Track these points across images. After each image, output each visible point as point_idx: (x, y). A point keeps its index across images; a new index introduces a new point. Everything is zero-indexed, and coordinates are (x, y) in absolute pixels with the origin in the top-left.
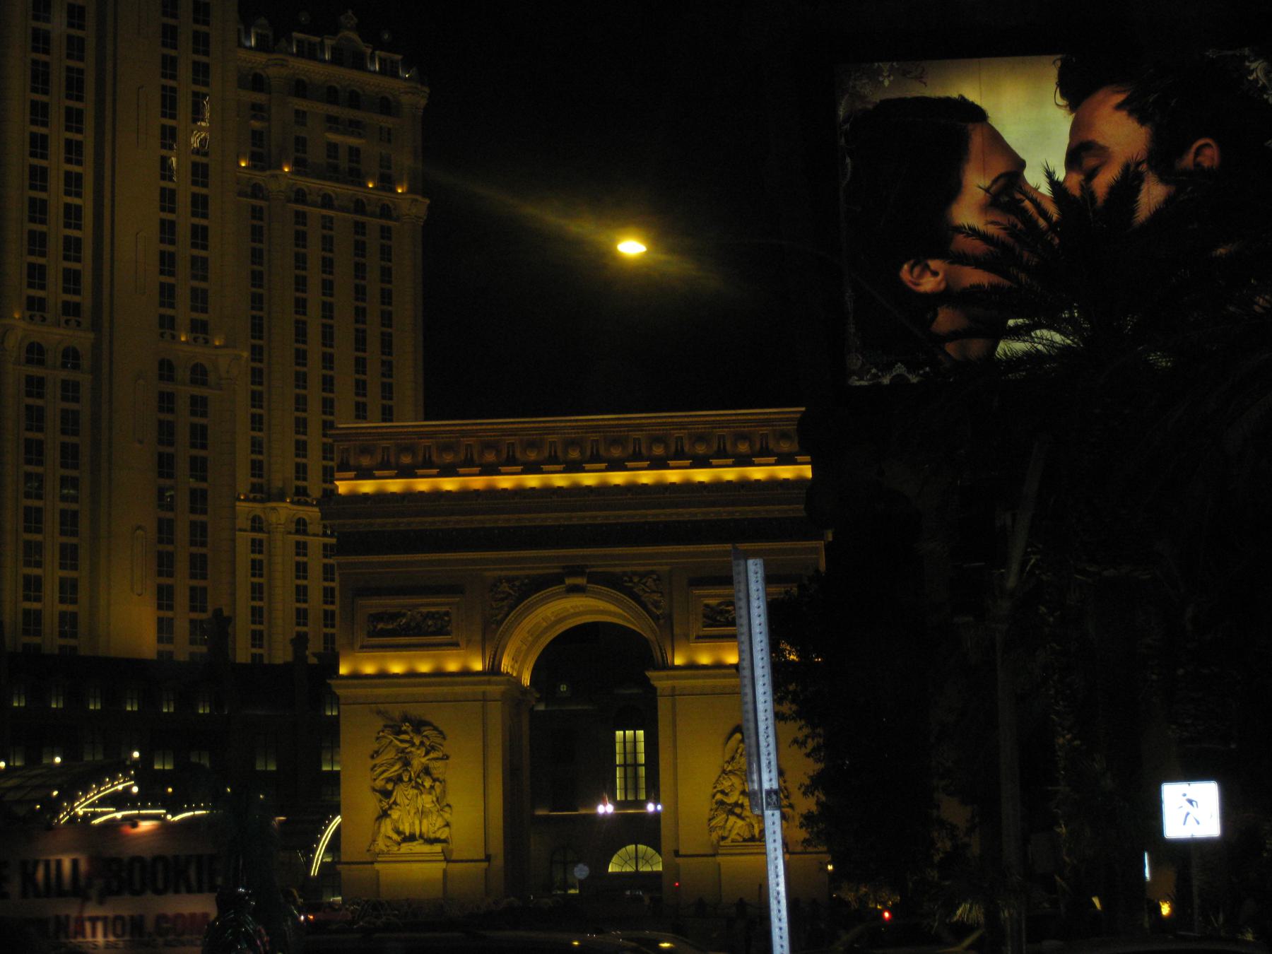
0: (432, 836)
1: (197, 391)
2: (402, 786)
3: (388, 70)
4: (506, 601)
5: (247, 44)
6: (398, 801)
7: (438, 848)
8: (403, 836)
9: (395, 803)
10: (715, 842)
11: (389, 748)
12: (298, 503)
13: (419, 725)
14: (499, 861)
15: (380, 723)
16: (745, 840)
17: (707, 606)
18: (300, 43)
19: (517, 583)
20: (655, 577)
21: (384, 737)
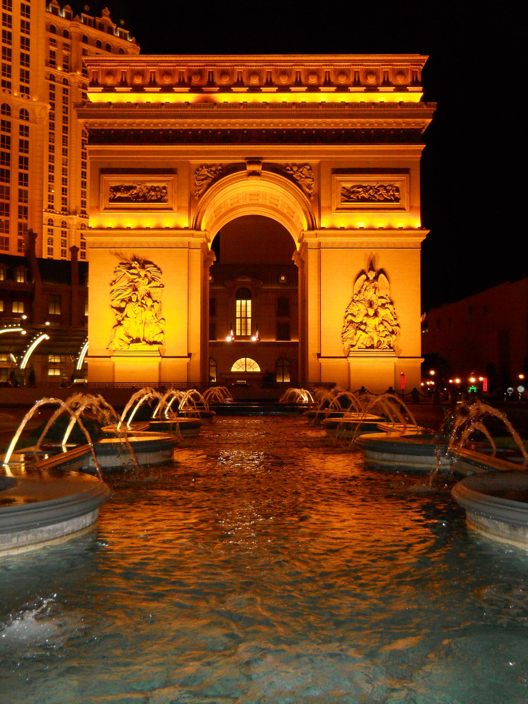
0: (152, 340)
1: (24, 123)
2: (131, 305)
3: (123, 36)
4: (205, 181)
5: (61, 16)
6: (128, 315)
7: (155, 347)
8: (132, 339)
9: (126, 316)
10: (346, 349)
11: (123, 279)
12: (82, 217)
13: (144, 263)
14: (197, 358)
15: (117, 261)
16: (367, 348)
17: (344, 188)
18: (85, 19)
19: (214, 169)
20: (308, 168)
21: (120, 271)
